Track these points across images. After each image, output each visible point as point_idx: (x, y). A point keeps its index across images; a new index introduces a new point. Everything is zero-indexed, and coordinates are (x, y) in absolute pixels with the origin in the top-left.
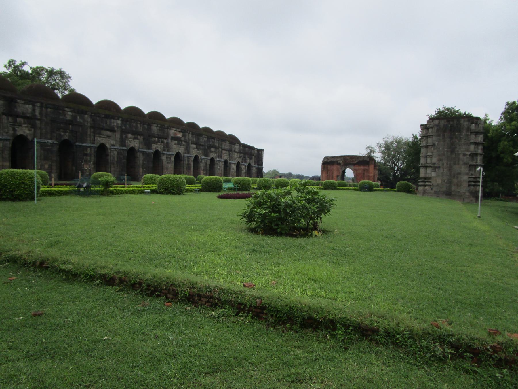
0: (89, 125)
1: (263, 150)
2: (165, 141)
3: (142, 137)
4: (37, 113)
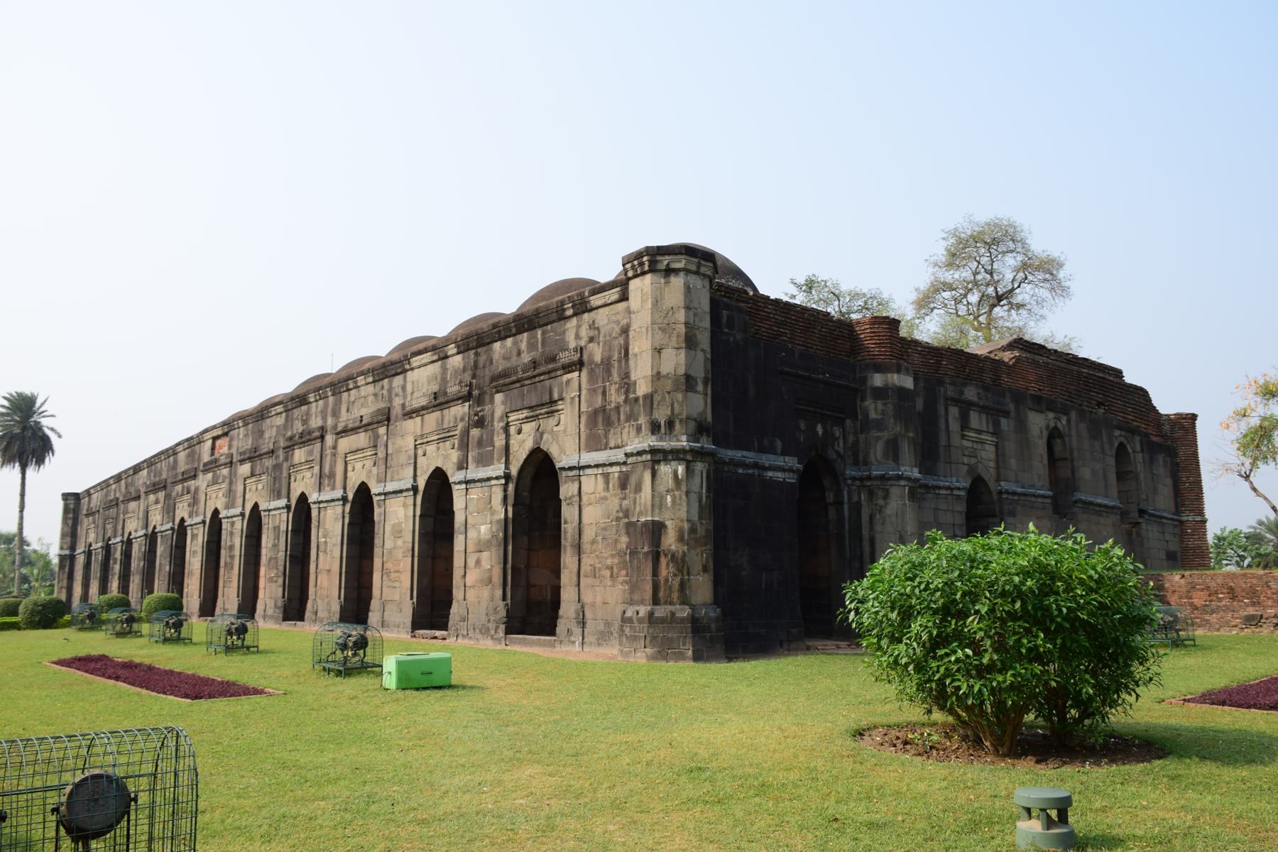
2: (192, 483)
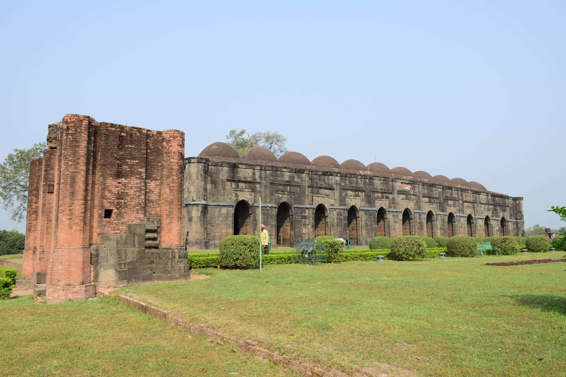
0: (307, 184)
1: (522, 199)
2: (391, 196)
3: (364, 193)
4: (257, 177)
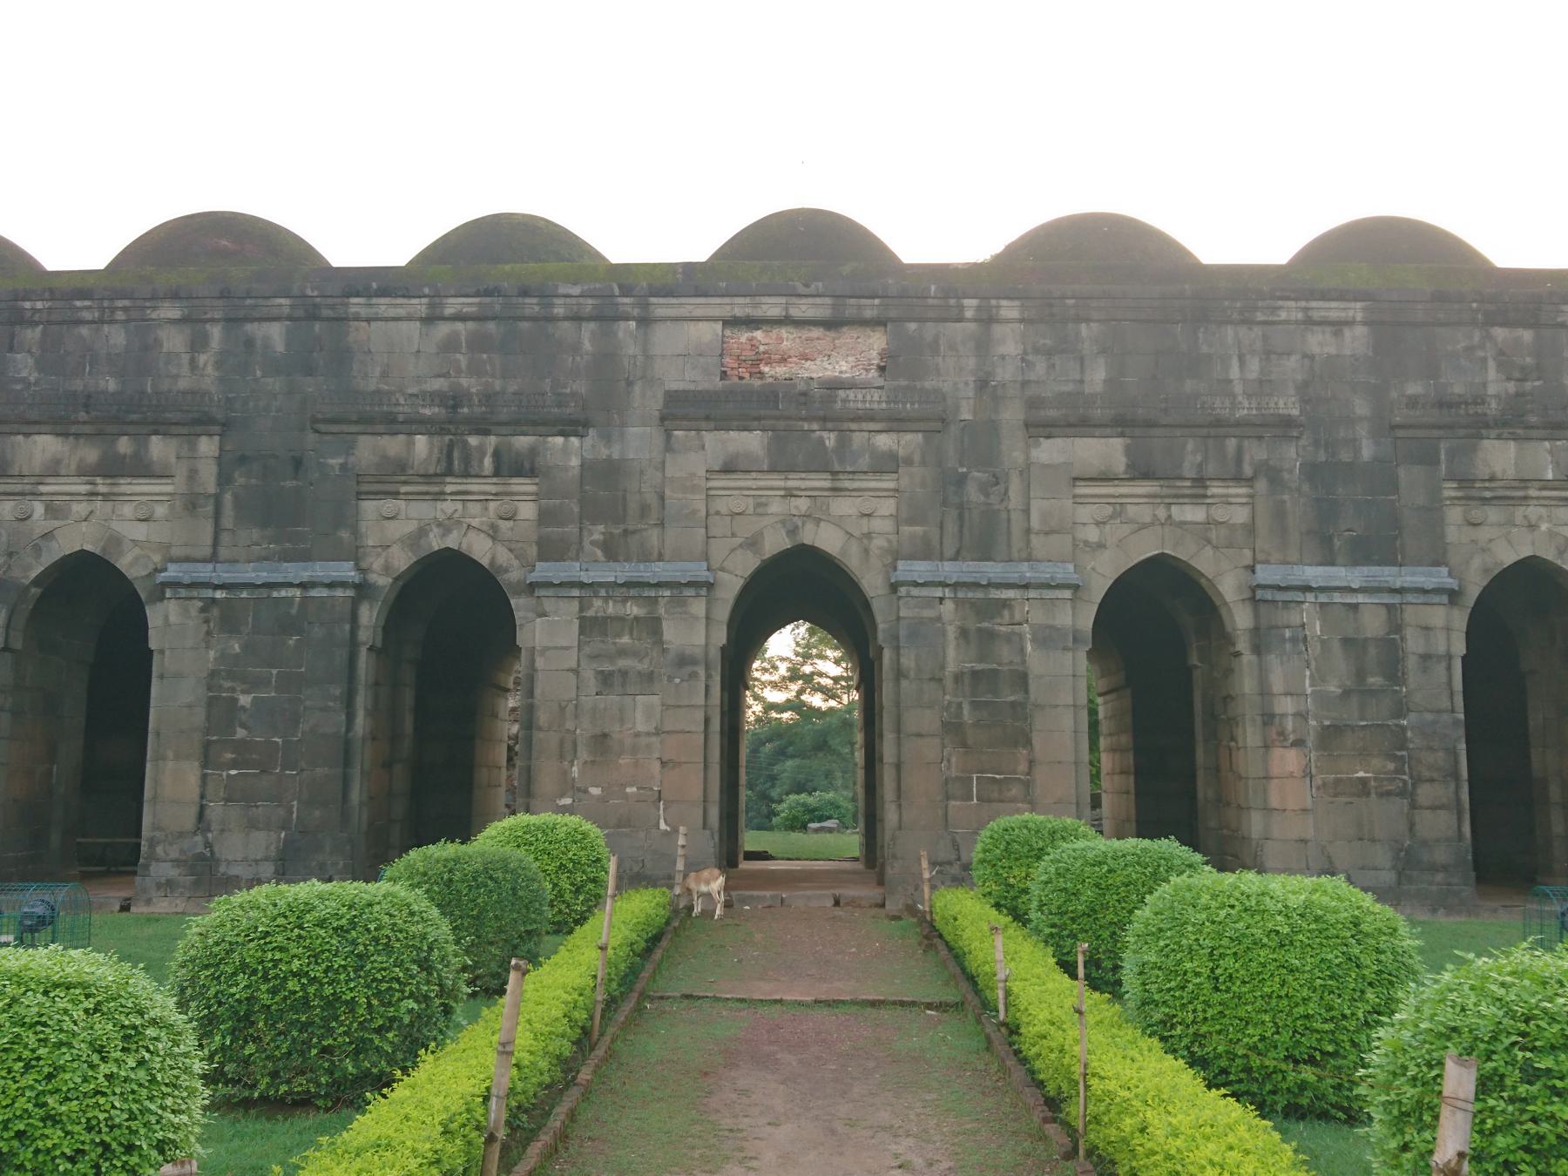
2: (567, 453)
3: (207, 446)
